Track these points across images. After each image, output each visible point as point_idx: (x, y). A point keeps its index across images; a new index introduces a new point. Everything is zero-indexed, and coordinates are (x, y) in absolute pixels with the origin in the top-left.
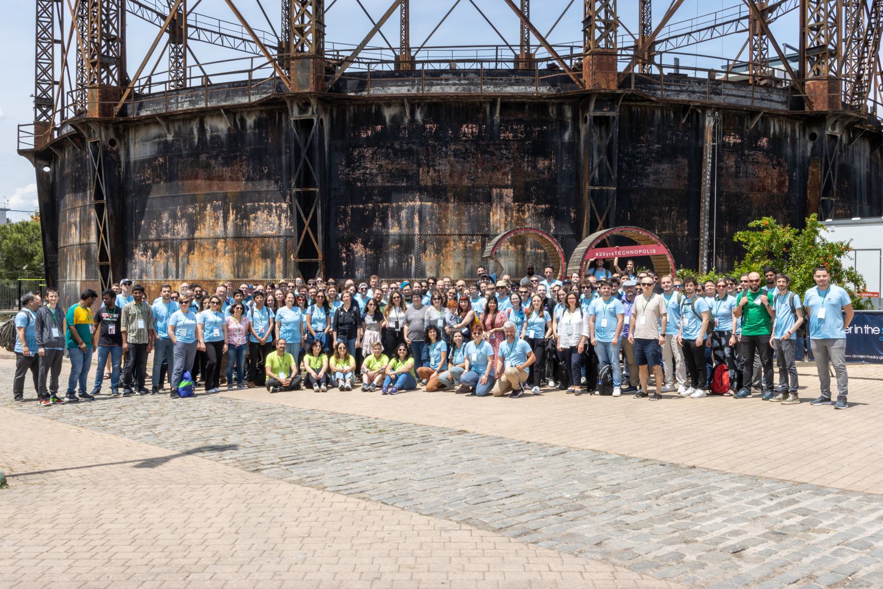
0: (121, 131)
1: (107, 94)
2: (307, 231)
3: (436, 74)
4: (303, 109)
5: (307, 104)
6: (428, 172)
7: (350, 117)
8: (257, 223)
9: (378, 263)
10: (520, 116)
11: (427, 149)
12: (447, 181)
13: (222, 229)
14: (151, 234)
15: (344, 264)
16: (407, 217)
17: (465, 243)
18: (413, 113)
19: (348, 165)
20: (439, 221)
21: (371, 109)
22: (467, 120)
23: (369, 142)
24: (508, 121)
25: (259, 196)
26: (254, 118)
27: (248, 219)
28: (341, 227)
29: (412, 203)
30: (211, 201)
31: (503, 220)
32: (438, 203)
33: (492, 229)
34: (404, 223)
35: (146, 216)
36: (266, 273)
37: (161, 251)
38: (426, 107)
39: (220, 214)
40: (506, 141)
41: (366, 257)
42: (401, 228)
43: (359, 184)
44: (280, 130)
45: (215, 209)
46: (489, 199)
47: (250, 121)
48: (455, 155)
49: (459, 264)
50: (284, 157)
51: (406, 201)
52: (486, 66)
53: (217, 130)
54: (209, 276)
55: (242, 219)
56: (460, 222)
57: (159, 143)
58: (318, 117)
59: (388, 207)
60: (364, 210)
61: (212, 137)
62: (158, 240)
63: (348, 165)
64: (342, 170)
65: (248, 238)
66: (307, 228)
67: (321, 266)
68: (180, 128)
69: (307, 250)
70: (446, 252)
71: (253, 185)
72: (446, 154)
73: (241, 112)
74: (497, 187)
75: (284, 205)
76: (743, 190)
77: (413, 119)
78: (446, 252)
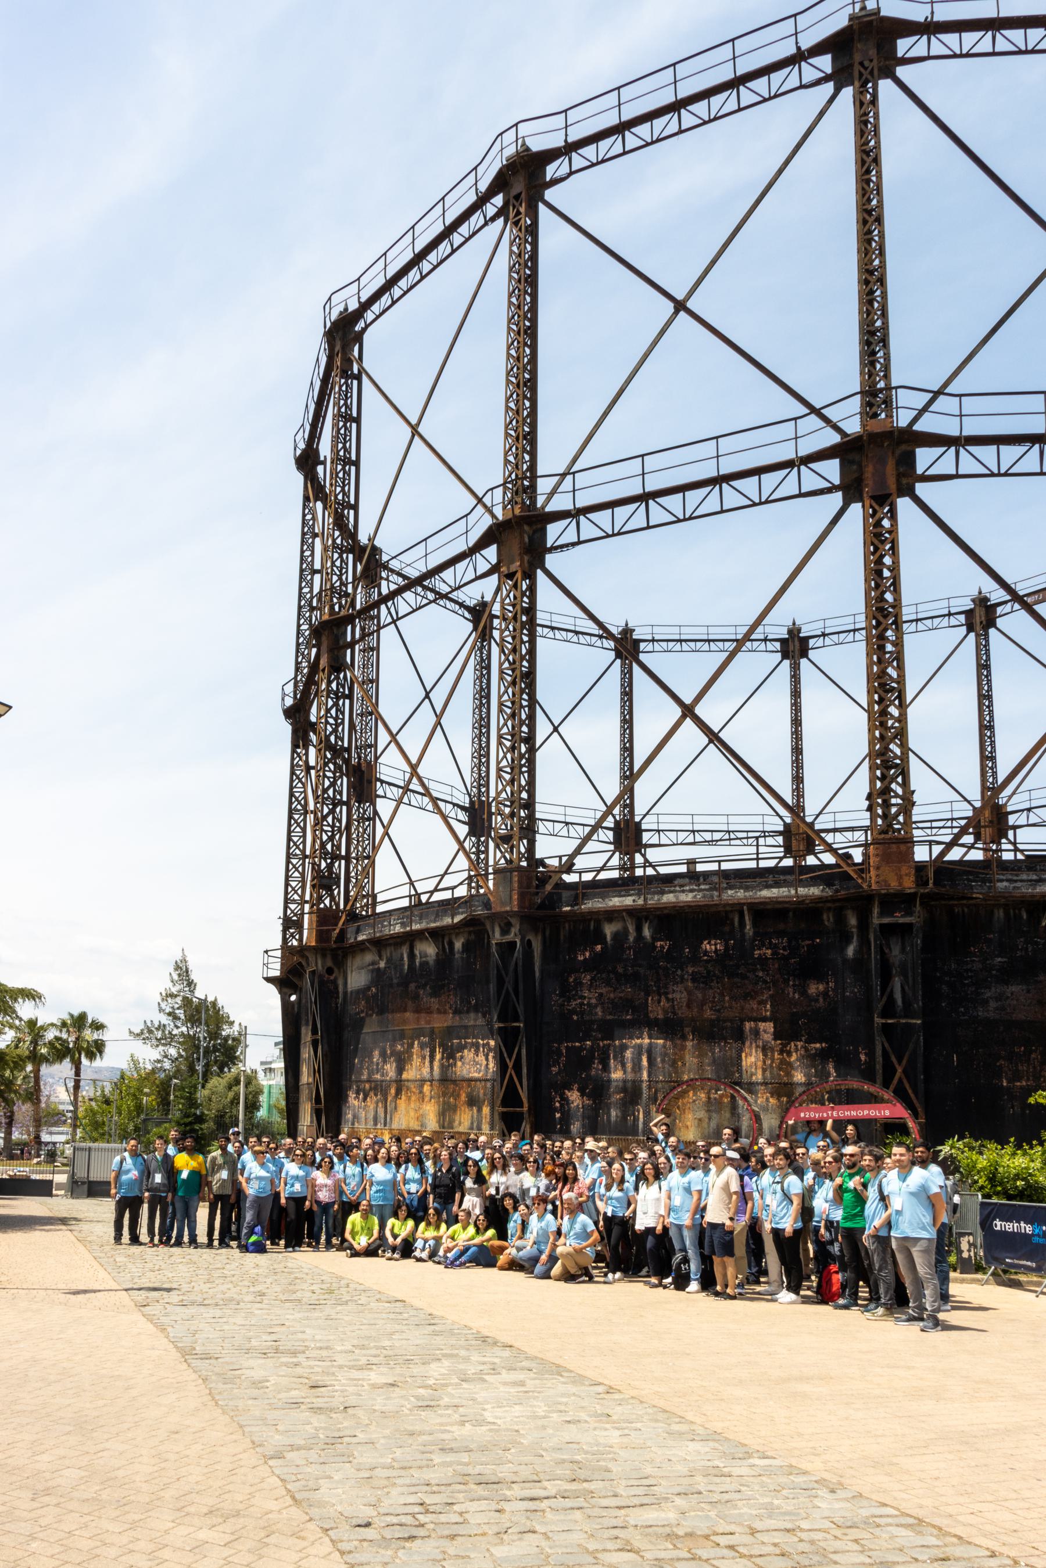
4: (505, 930)
6: (659, 1002)
8: (463, 1064)
9: (597, 1115)
12: (683, 1012)
13: (428, 1070)
14: (363, 1074)
15: (558, 1115)
16: (633, 1059)
17: (709, 1093)
18: (639, 929)
19: (561, 995)
20: (674, 1063)
21: (589, 926)
23: (587, 966)
25: (465, 1032)
26: (462, 940)
27: (454, 1058)
28: (555, 1069)
29: (639, 1041)
30: (418, 1037)
32: (672, 1040)
33: (744, 1076)
34: (629, 1066)
35: (359, 1054)
37: (372, 1094)
41: (583, 1107)
42: (625, 1072)
43: (575, 1018)
45: (422, 1046)
47: (458, 945)
49: (700, 1120)
50: (491, 986)
51: (631, 1038)
52: (725, 866)
53: (426, 956)
55: (448, 1059)
56: (701, 1066)
57: (372, 971)
59: (609, 1045)
60: (581, 1049)
61: (421, 964)
62: (369, 1081)
63: (561, 995)
65: (454, 1082)
70: (683, 1104)
71: (461, 1018)
72: (682, 977)
73: (450, 934)
75: (492, 1043)
78: (683, 1104)
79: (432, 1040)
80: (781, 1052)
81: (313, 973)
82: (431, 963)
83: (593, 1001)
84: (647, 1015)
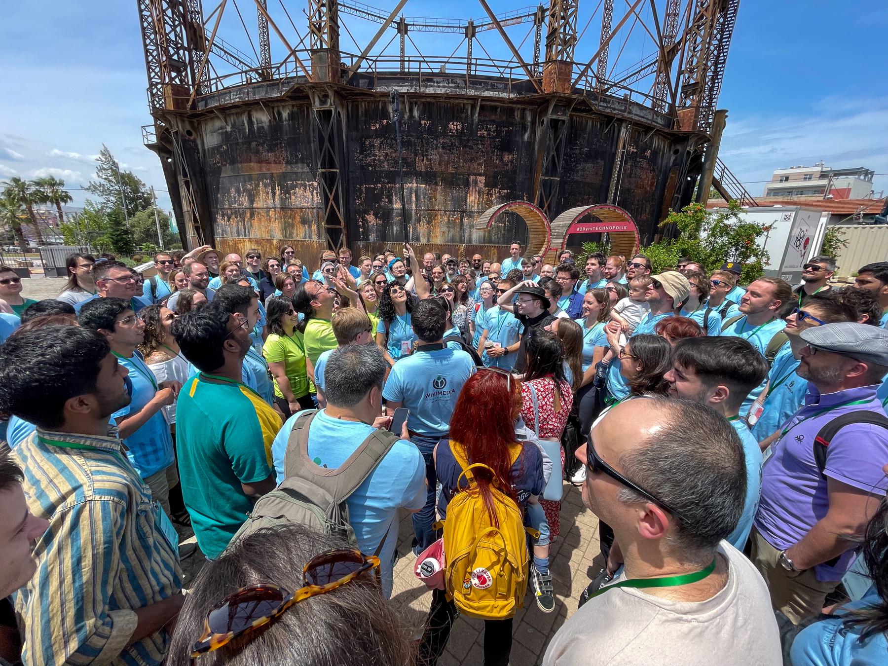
0: (196, 125)
1: (179, 92)
2: (332, 205)
3: (429, 78)
4: (323, 102)
5: (326, 96)
6: (423, 161)
7: (362, 112)
8: (296, 197)
9: (385, 230)
10: (493, 117)
11: (422, 142)
12: (436, 168)
15: (361, 230)
18: (411, 110)
19: (361, 153)
20: (430, 199)
21: (378, 106)
22: (453, 120)
23: (379, 134)
24: (484, 121)
25: (296, 176)
27: (290, 194)
29: (410, 185)
31: (476, 200)
35: (220, 192)
36: (305, 235)
37: (233, 216)
38: (422, 106)
39: (270, 189)
40: (482, 137)
43: (370, 169)
44: (308, 123)
45: (266, 186)
46: (467, 184)
47: (285, 115)
48: (443, 148)
50: (312, 144)
53: (262, 122)
54: (266, 236)
55: (285, 195)
56: (445, 201)
57: (222, 134)
58: (336, 109)
60: (375, 189)
61: (258, 128)
63: (361, 153)
64: (357, 156)
66: (331, 202)
67: (344, 232)
68: (234, 120)
69: (332, 219)
71: (292, 167)
72: (437, 145)
74: (473, 174)
75: (315, 184)
76: (633, 187)
77: (411, 116)
79: (272, 180)
80: (487, 195)
81: (176, 133)
82: (266, 127)
83: (382, 158)
84: (415, 169)
